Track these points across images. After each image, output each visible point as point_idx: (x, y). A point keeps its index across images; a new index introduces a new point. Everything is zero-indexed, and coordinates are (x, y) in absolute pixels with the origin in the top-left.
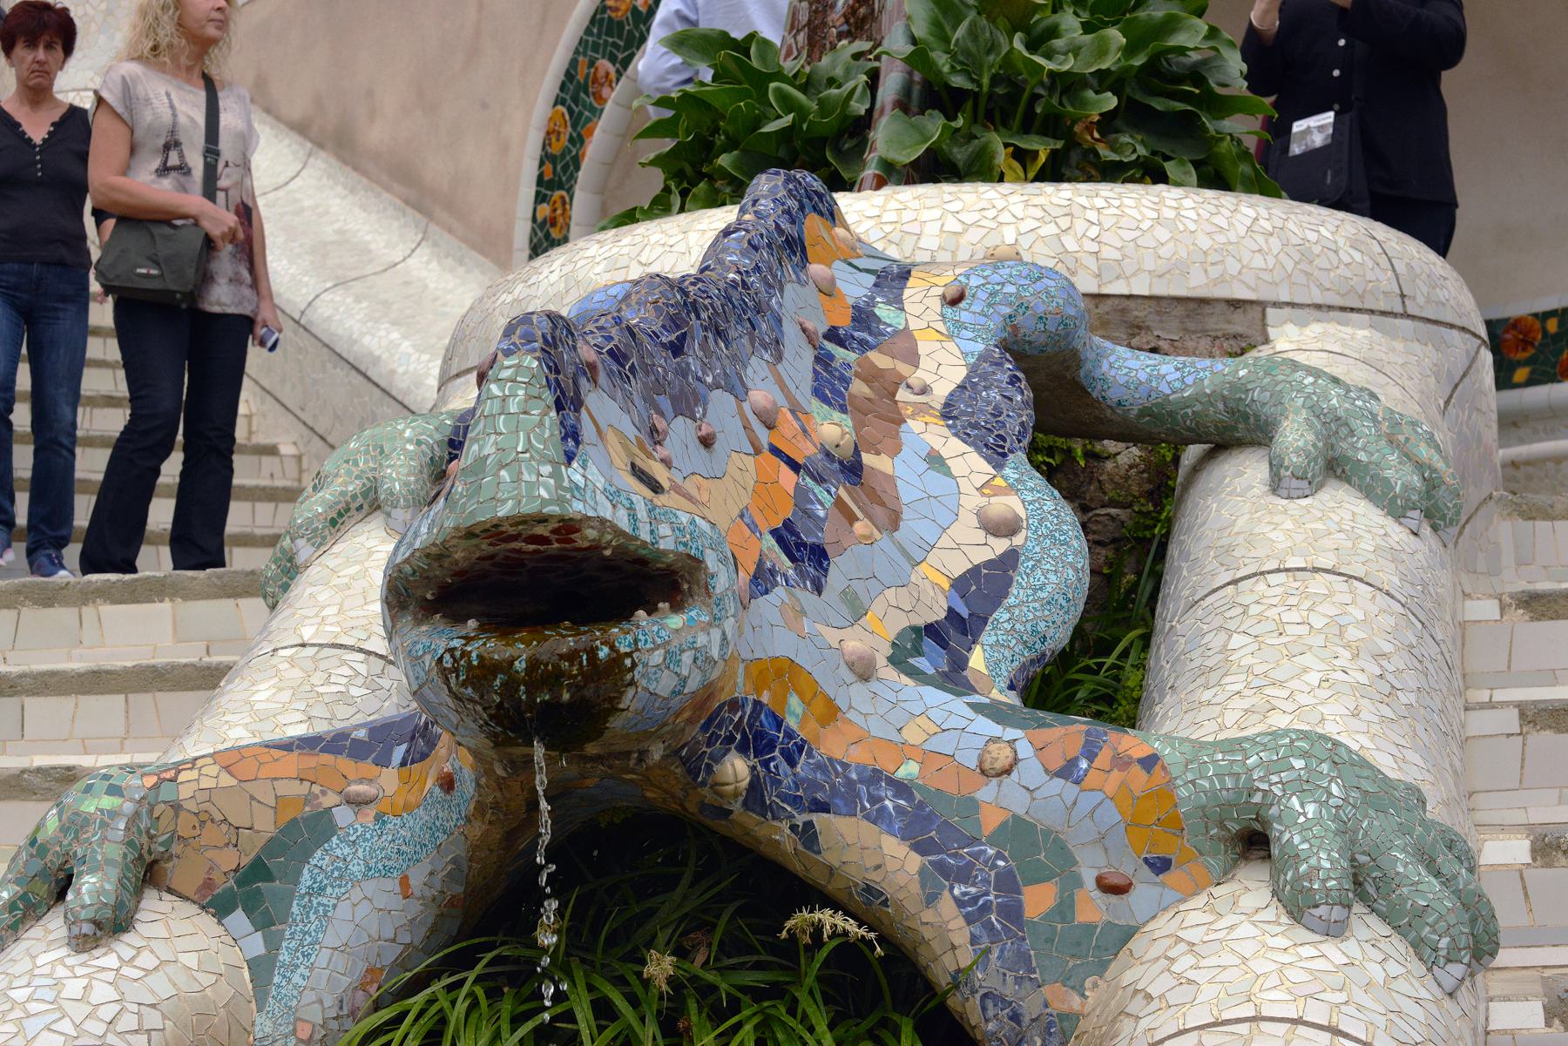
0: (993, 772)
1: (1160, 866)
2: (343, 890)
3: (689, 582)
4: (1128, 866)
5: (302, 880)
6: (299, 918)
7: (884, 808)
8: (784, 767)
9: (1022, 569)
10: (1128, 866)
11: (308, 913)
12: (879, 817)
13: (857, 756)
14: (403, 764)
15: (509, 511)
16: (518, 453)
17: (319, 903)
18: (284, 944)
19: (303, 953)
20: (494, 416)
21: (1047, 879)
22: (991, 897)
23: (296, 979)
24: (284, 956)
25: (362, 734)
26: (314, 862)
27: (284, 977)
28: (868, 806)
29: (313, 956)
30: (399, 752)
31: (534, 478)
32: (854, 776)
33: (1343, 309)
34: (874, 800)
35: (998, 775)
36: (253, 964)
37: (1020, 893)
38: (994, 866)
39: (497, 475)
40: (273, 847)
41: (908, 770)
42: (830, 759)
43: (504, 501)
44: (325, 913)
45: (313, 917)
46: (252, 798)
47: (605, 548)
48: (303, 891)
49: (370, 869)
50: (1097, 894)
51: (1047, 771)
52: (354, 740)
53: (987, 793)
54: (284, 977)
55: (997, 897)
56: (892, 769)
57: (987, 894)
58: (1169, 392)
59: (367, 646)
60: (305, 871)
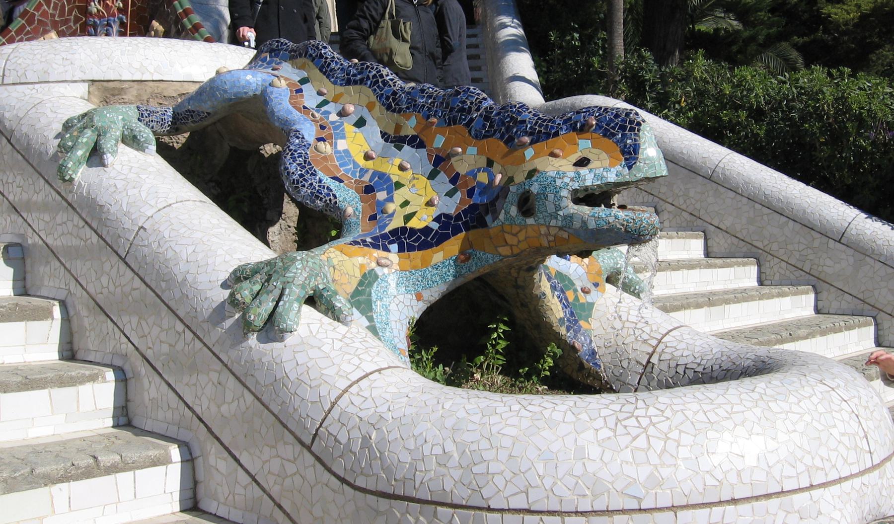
1: (596, 285)
2: (391, 299)
4: (589, 285)
5: (372, 295)
10: (589, 285)
17: (383, 304)
18: (375, 320)
21: (570, 289)
23: (388, 334)
24: (378, 325)
26: (375, 289)
29: (390, 325)
30: (394, 247)
36: (367, 328)
40: (361, 283)
43: (664, 170)
44: (387, 308)
45: (382, 310)
50: (582, 294)
52: (370, 242)
60: (373, 292)
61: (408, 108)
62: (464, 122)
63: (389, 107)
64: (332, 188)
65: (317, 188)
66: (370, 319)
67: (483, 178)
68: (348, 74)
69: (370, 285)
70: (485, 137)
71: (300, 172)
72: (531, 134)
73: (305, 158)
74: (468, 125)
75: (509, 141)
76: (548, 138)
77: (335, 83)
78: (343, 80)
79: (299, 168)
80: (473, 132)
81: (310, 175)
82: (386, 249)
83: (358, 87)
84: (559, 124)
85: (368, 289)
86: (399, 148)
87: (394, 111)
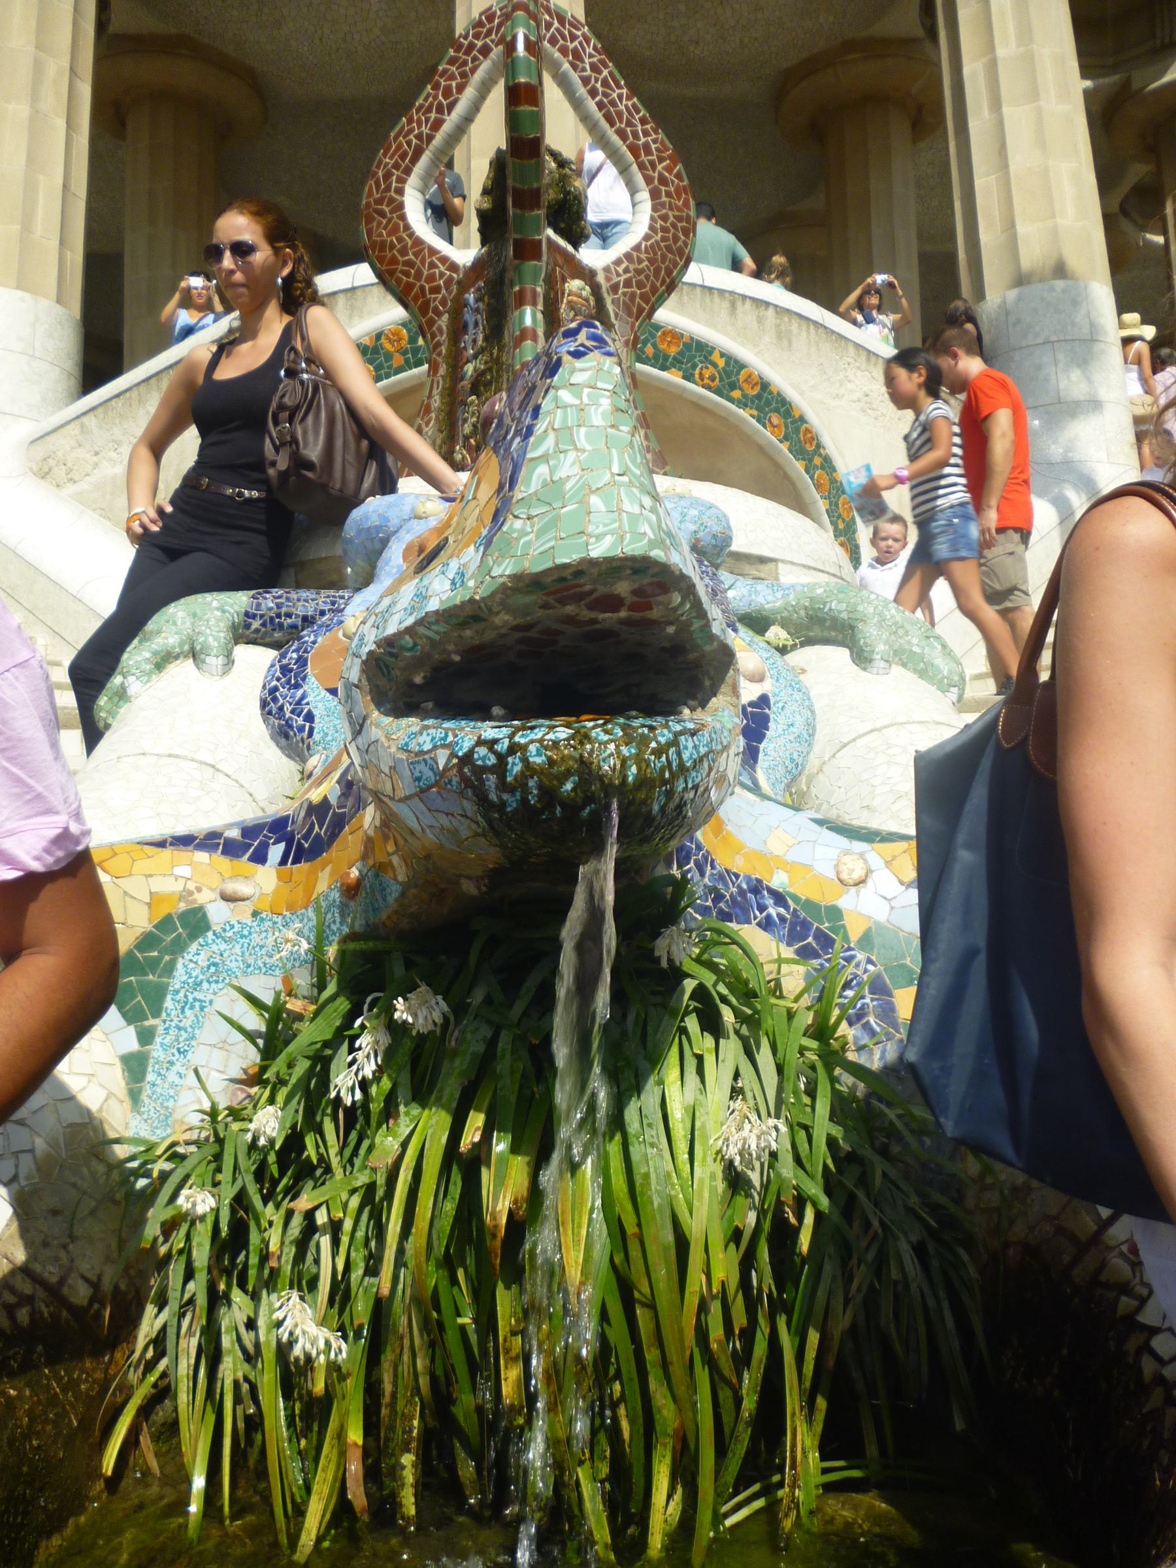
0: (851, 882)
3: (711, 678)
6: (173, 1013)
7: (769, 917)
8: (697, 876)
9: (774, 708)
11: (183, 1008)
12: (767, 925)
13: (739, 865)
14: (283, 862)
15: (609, 550)
16: (613, 474)
17: (195, 999)
18: (158, 1040)
19: (178, 1050)
20: (570, 428)
22: (867, 1000)
23: (172, 1077)
25: (234, 834)
26: (190, 956)
27: (159, 1074)
28: (757, 913)
30: (276, 852)
31: (636, 510)
32: (744, 886)
33: (815, 569)
34: (762, 908)
35: (856, 885)
37: (891, 995)
38: (866, 971)
39: (584, 502)
41: (778, 881)
42: (727, 871)
43: (599, 537)
44: (202, 1008)
45: (188, 1012)
46: (125, 893)
47: (671, 623)
48: (177, 986)
49: (249, 966)
51: (902, 883)
53: (845, 902)
54: (159, 1074)
55: (872, 1000)
56: (768, 877)
57: (863, 997)
58: (764, 602)
59: (199, 757)
60: (179, 965)
64: (315, 712)
65: (288, 715)
66: (146, 1037)
69: (178, 948)
71: (274, 683)
73: (306, 651)
79: (278, 674)
81: (289, 689)
82: (260, 857)
85: (167, 958)
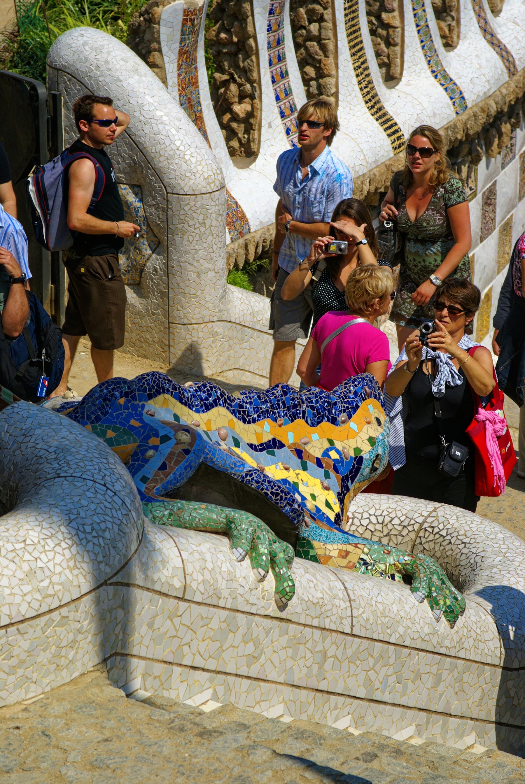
61: (259, 416)
62: (301, 416)
63: (244, 421)
67: (334, 455)
68: (202, 399)
70: (319, 423)
72: (344, 411)
74: (303, 417)
75: (334, 421)
76: (355, 411)
77: (197, 411)
78: (201, 407)
80: (310, 422)
83: (215, 410)
84: (353, 398)
86: (273, 454)
87: (249, 422)
